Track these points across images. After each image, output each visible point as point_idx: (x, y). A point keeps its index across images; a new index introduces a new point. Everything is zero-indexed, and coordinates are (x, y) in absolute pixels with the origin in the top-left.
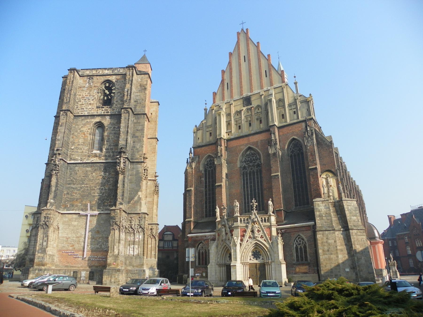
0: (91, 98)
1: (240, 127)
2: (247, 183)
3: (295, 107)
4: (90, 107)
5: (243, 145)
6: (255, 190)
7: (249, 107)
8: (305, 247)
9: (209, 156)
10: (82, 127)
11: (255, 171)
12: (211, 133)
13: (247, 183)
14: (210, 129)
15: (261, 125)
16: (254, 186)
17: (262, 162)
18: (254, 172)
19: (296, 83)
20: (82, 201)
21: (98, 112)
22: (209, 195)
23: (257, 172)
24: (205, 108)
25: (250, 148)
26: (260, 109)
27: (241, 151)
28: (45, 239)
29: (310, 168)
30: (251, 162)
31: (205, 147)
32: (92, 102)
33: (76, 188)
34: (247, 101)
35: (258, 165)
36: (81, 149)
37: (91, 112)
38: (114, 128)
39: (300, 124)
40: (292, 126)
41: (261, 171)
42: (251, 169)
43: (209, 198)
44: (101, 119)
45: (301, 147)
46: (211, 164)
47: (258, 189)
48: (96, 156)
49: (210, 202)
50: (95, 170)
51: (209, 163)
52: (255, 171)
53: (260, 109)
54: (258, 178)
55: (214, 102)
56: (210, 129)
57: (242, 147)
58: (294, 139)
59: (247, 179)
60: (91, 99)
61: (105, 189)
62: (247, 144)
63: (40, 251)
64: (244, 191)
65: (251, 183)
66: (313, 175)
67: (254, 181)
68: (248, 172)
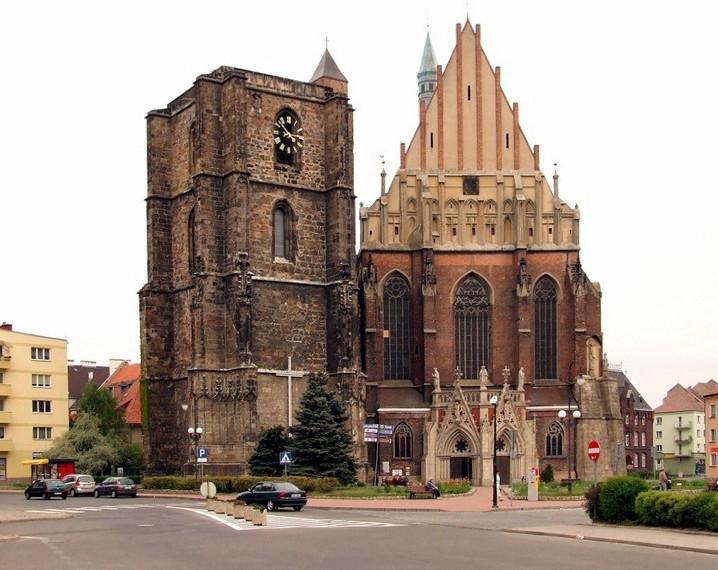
0: (263, 144)
1: (454, 229)
2: (462, 331)
3: (552, 221)
4: (262, 164)
5: (462, 267)
6: (474, 345)
7: (474, 197)
8: (560, 437)
9: (396, 272)
10: (255, 207)
11: (477, 314)
12: (397, 228)
13: (462, 331)
14: (396, 220)
15: (493, 237)
16: (474, 340)
17: (493, 302)
18: (474, 317)
19: (555, 178)
20: (273, 352)
21: (278, 180)
22: (393, 342)
23: (480, 317)
24: (381, 171)
25: (472, 275)
26: (493, 207)
27: (457, 276)
28: (253, 418)
29: (577, 330)
30: (471, 298)
31: (388, 255)
32: (265, 154)
33: (260, 328)
34: (471, 184)
35: (483, 306)
36: (258, 252)
37: (266, 176)
38: (309, 217)
39: (561, 254)
40: (546, 255)
41: (486, 317)
42: (471, 310)
43: (393, 348)
44: (284, 194)
45: (554, 290)
46: (396, 287)
47: (480, 345)
48: (284, 269)
49: (393, 356)
50: (288, 297)
51: (394, 284)
52: (477, 314)
53: (493, 207)
54: (480, 325)
55: (403, 166)
56: (396, 220)
57: (460, 270)
58: (546, 275)
59: (462, 325)
60: (263, 147)
61: (306, 334)
62: (470, 267)
63: (248, 438)
64: (457, 345)
65: (468, 332)
66: (580, 342)
67: (474, 330)
68: (465, 314)
